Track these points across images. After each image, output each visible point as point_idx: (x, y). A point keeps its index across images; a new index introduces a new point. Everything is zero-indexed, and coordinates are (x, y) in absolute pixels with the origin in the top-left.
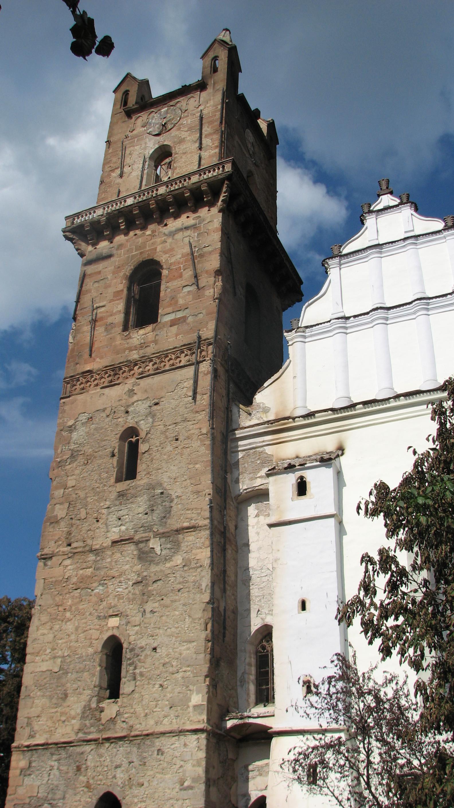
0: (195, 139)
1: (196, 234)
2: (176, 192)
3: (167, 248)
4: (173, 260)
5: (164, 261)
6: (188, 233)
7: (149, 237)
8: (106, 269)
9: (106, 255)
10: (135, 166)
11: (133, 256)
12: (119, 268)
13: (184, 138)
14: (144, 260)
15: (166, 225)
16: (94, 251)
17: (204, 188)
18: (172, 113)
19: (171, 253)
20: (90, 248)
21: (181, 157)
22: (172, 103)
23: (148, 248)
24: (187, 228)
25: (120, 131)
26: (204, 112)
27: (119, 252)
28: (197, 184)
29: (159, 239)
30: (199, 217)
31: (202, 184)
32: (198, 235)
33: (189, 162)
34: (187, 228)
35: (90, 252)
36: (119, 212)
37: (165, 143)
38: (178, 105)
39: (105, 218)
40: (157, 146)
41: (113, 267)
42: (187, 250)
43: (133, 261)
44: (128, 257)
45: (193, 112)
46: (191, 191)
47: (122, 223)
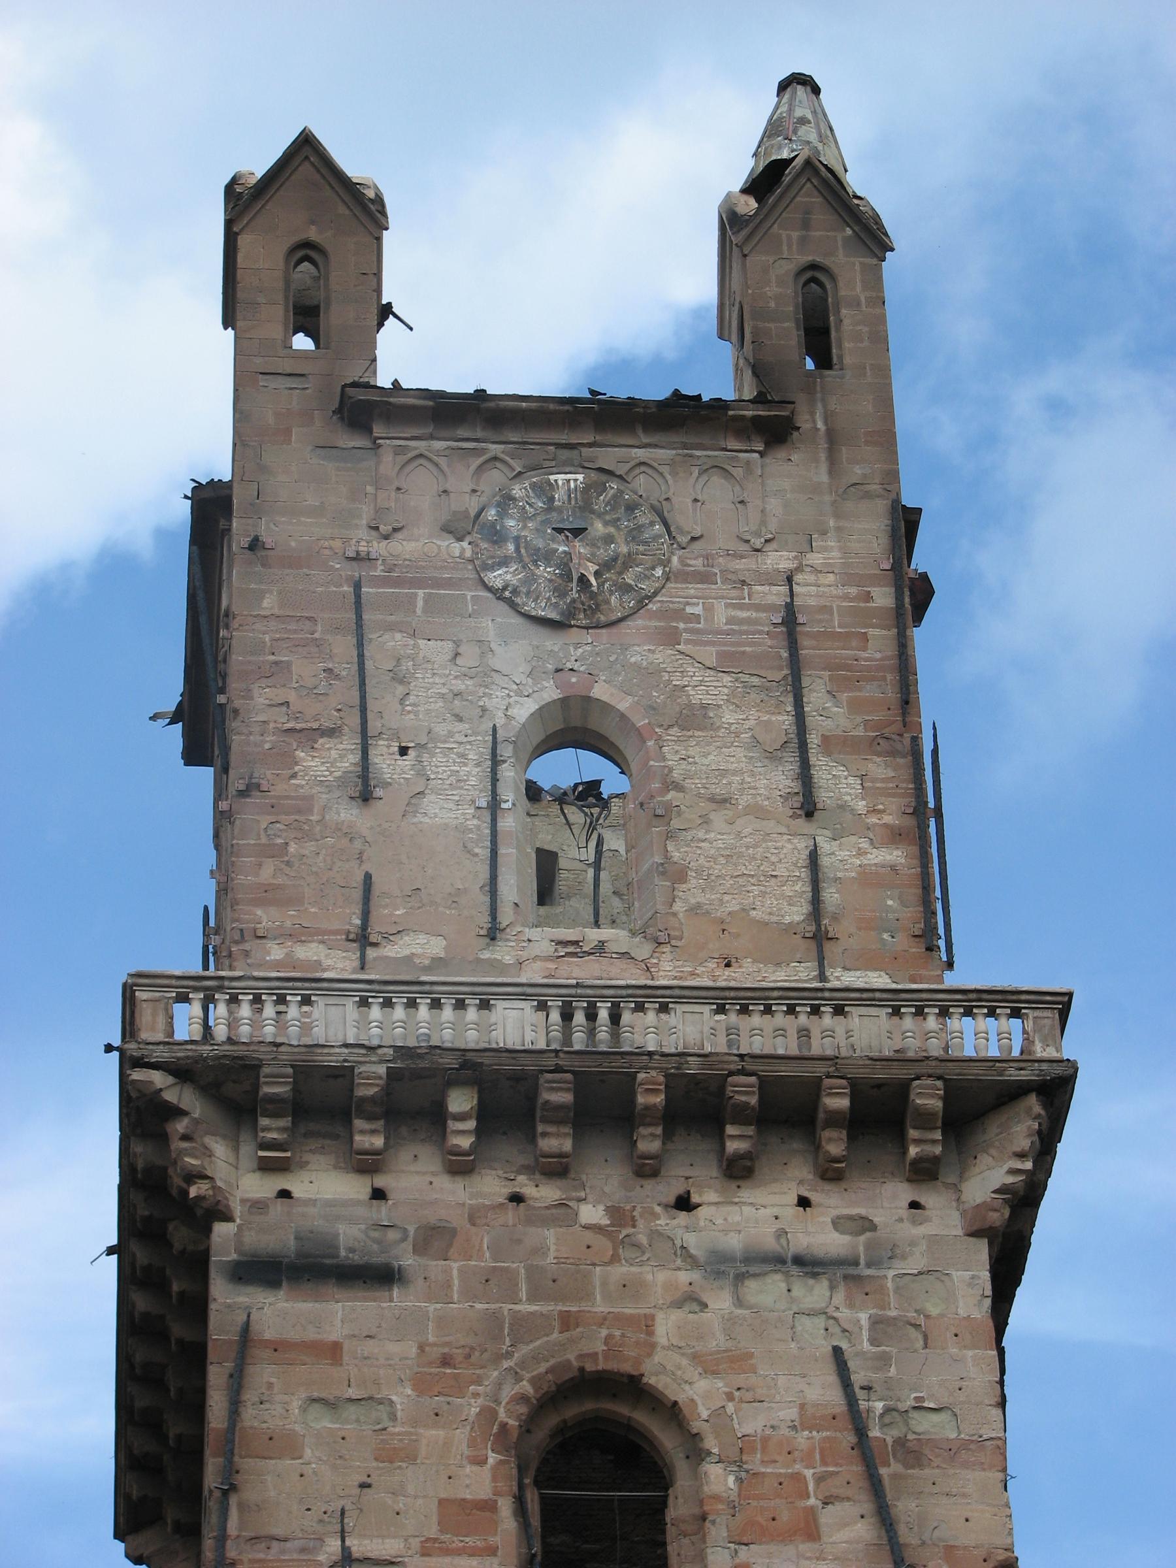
0: (773, 740)
1: (864, 1317)
2: (785, 1070)
3: (712, 1345)
4: (751, 1424)
5: (705, 1414)
6: (815, 1293)
7: (603, 1245)
8: (370, 1347)
9: (356, 1258)
10: (439, 765)
11: (523, 1328)
12: (446, 1361)
13: (704, 707)
14: (590, 1367)
15: (684, 1204)
16: (280, 1206)
17: (928, 1098)
18: (615, 522)
19: (740, 1380)
20: (254, 1186)
21: (706, 821)
22: (608, 457)
23: (600, 1307)
24: (808, 1265)
25: (312, 501)
26: (807, 592)
27: (435, 1266)
28: (898, 1073)
29: (662, 1276)
30: (865, 1225)
31: (918, 1078)
32: (875, 1322)
33: (751, 869)
34: (808, 1265)
35: (258, 1206)
36: (465, 1065)
37: (600, 691)
38: (642, 482)
39: (382, 1070)
40: (551, 692)
41: (411, 1349)
42: (824, 1391)
43: (524, 1350)
44: (494, 1318)
45: (739, 565)
46: (857, 1088)
47: (461, 1117)
